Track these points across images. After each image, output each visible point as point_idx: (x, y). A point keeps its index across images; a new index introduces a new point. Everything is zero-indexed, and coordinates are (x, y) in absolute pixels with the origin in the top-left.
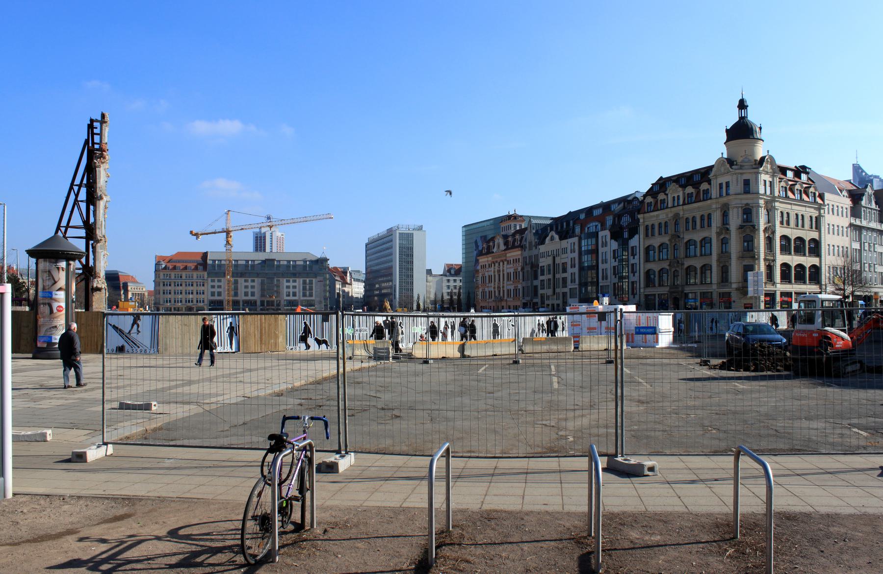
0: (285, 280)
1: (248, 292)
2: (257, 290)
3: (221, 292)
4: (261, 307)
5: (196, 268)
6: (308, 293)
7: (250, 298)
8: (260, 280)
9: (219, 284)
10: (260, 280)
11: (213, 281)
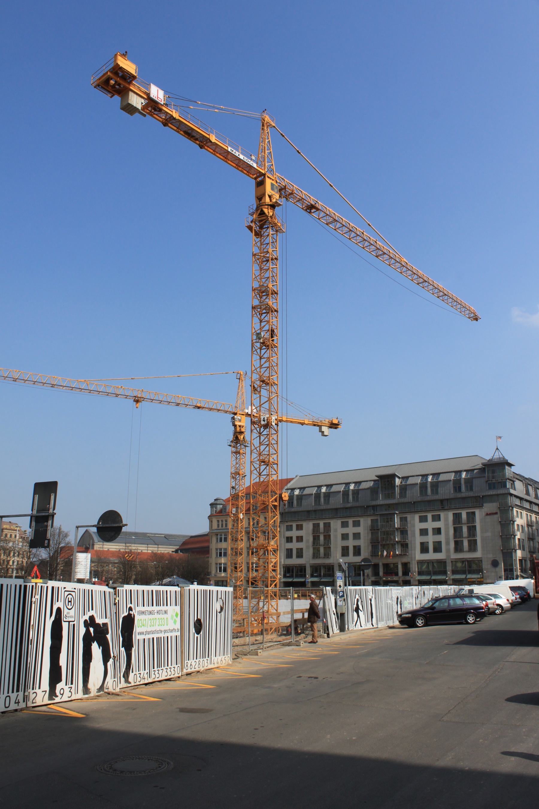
0: (417, 517)
1: (347, 547)
2: (364, 543)
3: (302, 549)
6: (466, 544)
11: (289, 528)
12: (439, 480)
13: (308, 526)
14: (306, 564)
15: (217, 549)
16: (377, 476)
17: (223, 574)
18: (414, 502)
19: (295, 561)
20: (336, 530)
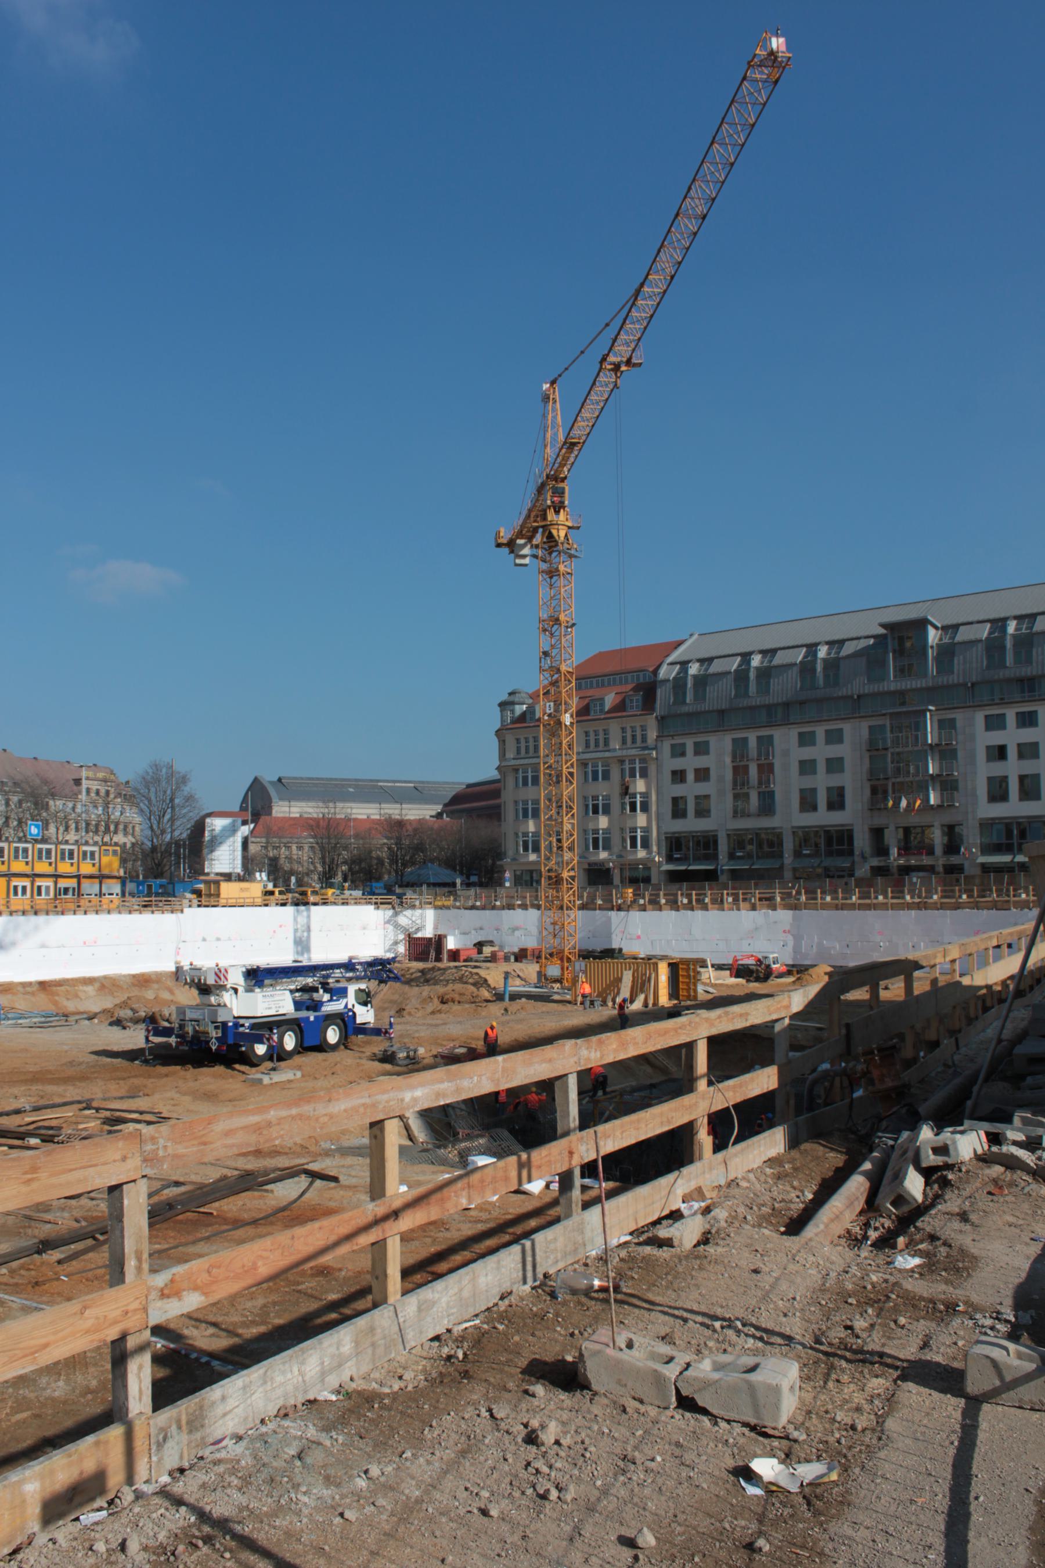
0: (979, 717)
3: (707, 797)
4: (875, 862)
5: (620, 707)
7: (823, 817)
8: (863, 728)
9: (702, 762)
10: (863, 728)
11: (679, 752)
12: (1035, 629)
13: (721, 745)
14: (716, 831)
15: (516, 802)
16: (883, 626)
17: (533, 857)
18: (973, 685)
19: (691, 824)
20: (786, 753)
